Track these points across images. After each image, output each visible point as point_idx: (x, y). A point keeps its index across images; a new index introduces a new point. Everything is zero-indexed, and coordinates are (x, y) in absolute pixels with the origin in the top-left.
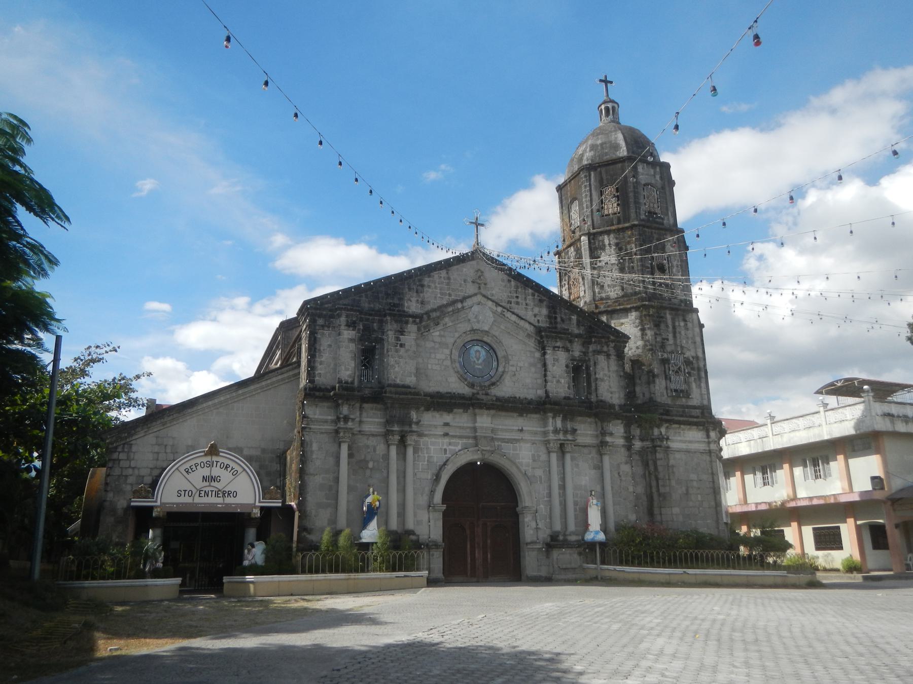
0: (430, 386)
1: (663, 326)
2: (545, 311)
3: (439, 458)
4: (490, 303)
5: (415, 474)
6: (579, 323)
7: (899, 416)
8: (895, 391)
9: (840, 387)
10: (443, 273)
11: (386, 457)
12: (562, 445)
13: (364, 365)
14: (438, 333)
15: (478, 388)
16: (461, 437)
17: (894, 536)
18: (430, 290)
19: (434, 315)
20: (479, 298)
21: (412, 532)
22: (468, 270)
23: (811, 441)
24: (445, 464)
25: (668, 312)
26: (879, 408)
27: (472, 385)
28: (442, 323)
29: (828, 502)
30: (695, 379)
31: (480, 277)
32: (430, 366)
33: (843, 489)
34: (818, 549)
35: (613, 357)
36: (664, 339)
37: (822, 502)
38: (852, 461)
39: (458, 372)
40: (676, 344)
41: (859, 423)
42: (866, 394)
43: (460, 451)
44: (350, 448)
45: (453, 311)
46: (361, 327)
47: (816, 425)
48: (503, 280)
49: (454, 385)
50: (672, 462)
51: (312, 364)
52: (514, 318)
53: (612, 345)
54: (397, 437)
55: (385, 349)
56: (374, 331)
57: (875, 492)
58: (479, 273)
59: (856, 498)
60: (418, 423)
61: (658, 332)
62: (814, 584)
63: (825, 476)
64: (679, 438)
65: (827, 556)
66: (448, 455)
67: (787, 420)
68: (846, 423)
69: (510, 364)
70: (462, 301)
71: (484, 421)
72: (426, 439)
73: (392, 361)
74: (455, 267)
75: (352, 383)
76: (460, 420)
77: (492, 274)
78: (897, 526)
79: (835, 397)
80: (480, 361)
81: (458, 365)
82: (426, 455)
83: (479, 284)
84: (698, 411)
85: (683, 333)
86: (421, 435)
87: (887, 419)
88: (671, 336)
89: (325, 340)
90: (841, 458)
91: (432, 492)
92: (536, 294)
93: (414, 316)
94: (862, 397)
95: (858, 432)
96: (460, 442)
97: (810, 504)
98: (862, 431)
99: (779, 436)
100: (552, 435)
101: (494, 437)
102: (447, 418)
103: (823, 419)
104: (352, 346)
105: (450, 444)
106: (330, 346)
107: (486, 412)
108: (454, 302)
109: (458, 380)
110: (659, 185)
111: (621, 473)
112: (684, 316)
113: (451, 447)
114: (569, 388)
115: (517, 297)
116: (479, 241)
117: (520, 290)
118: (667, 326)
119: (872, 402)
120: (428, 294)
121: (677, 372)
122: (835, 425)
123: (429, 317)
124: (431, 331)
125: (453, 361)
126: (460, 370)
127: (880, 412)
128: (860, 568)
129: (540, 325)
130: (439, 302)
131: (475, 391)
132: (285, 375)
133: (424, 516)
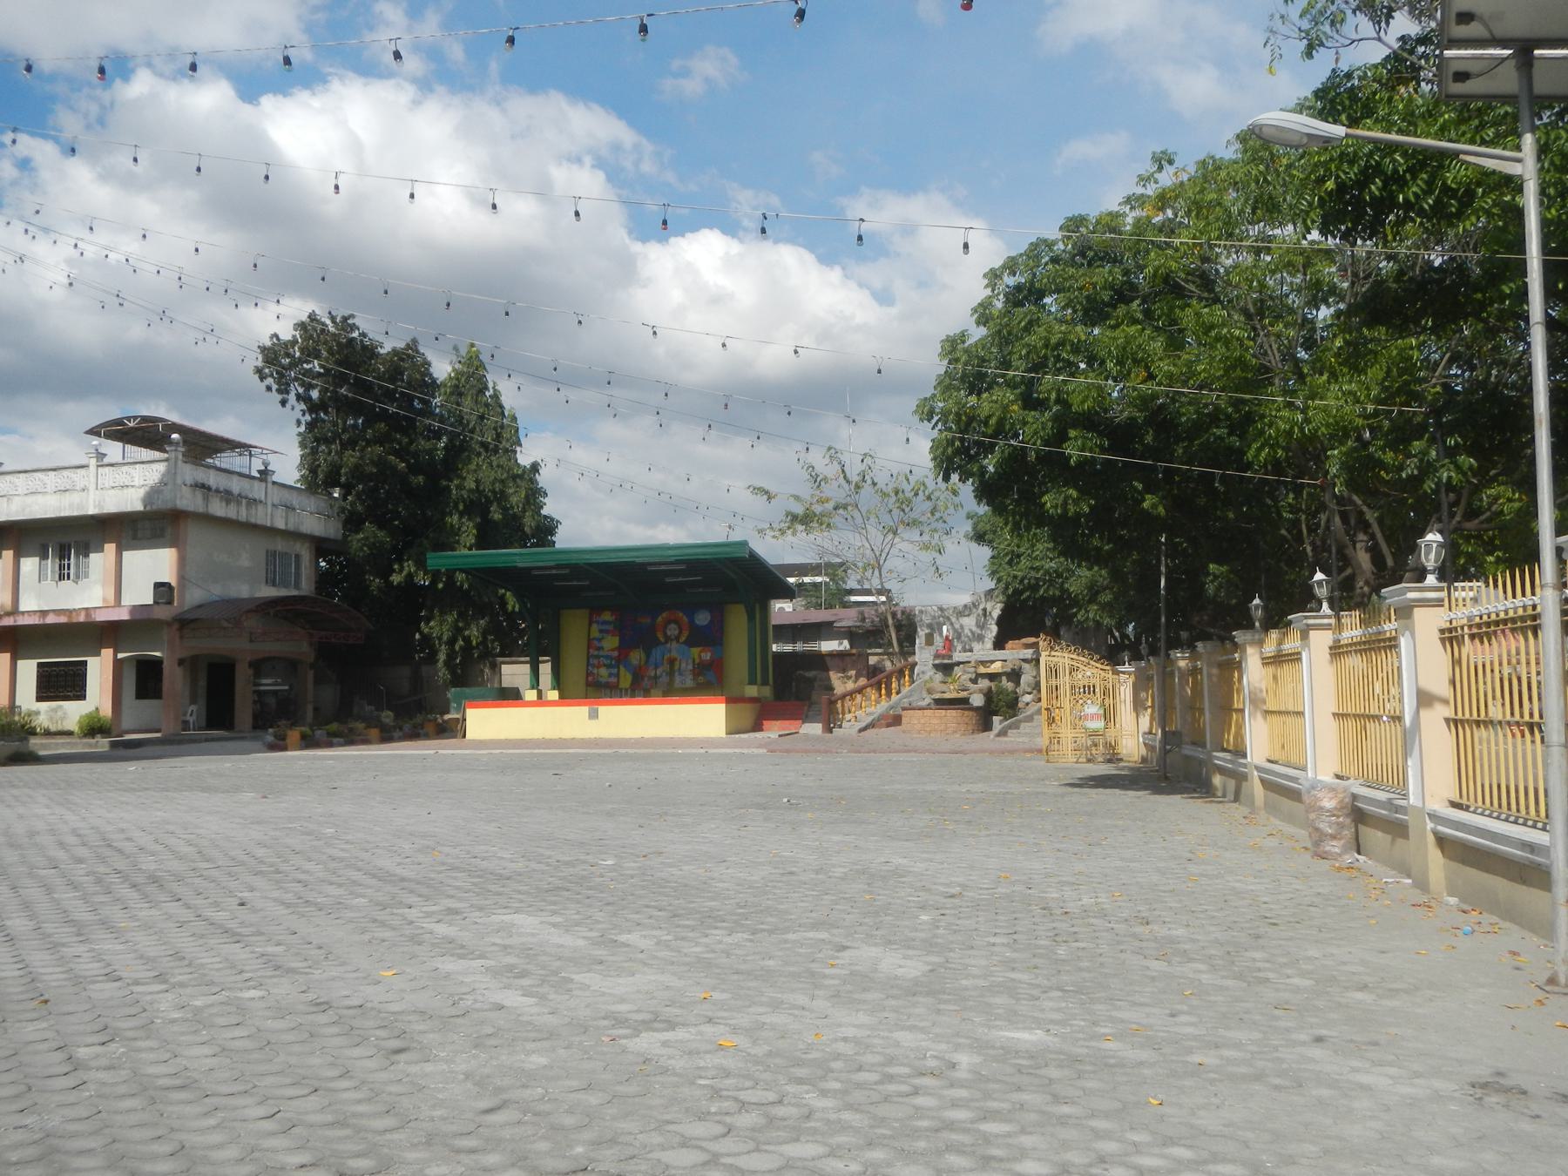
7: (217, 491)
8: (221, 451)
9: (132, 428)
17: (174, 678)
23: (62, 514)
26: (190, 473)
29: (75, 621)
33: (104, 600)
34: (41, 698)
37: (63, 619)
38: (126, 555)
41: (152, 494)
42: (173, 448)
47: (78, 488)
57: (156, 607)
59: (124, 615)
62: (24, 758)
63: (78, 577)
65: (55, 710)
67: (26, 472)
68: (133, 490)
78: (181, 662)
79: (121, 444)
87: (199, 494)
90: (110, 548)
94: (165, 451)
95: (148, 508)
97: (41, 622)
98: (154, 507)
99: (5, 499)
103: (93, 480)
119: (180, 462)
122: (113, 492)
127: (189, 481)
128: (109, 729)
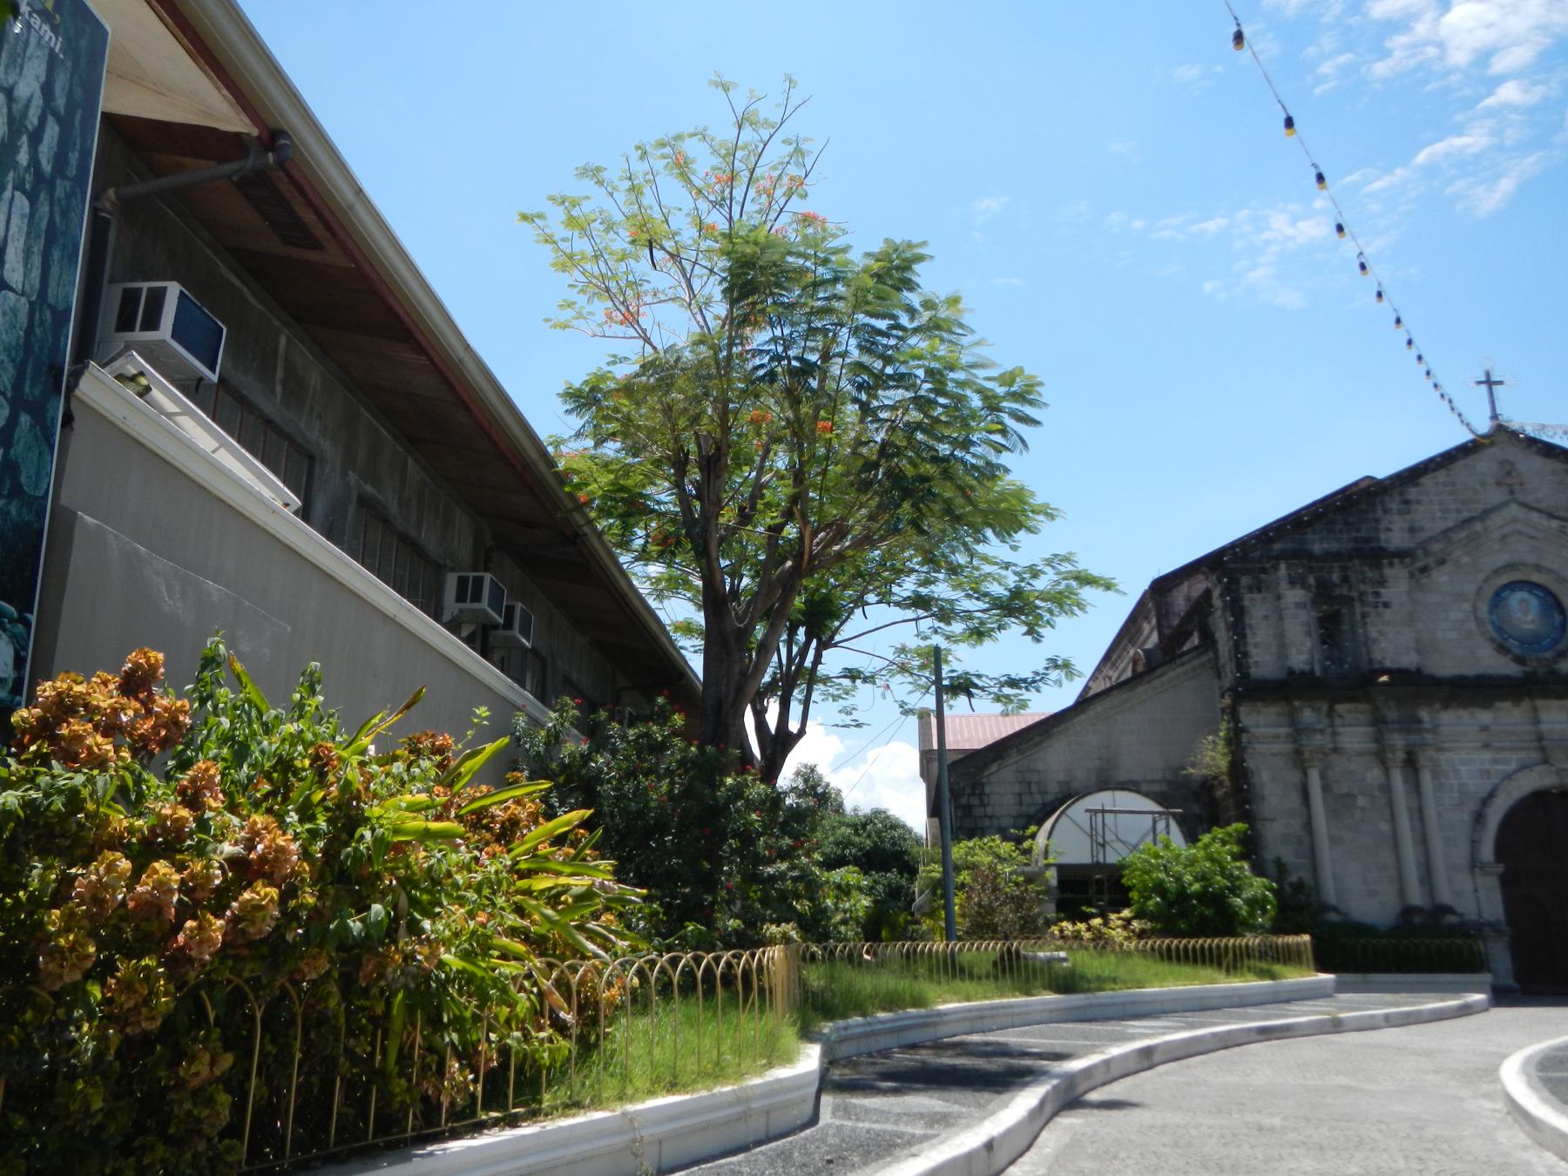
0: (1445, 666)
3: (1478, 787)
4: (1535, 516)
5: (1439, 814)
10: (1441, 476)
11: (1387, 788)
13: (1324, 643)
14: (1445, 578)
15: (1534, 664)
16: (1513, 749)
18: (1422, 508)
19: (1436, 547)
20: (1514, 510)
21: (1450, 910)
22: (1484, 464)
24: (1491, 795)
27: (1520, 660)
31: (1509, 473)
32: (1439, 635)
39: (1493, 640)
43: (1515, 772)
44: (1323, 776)
48: (1554, 473)
49: (1493, 663)
51: (1242, 649)
54: (1401, 755)
55: (1358, 617)
56: (1335, 585)
58: (1508, 467)
60: (1434, 730)
66: (1495, 781)
72: (1448, 755)
73: (1373, 632)
74: (1460, 463)
75: (1312, 671)
76: (1510, 716)
77: (1531, 465)
80: (1530, 617)
81: (1490, 627)
82: (1455, 782)
83: (1509, 485)
86: (1439, 749)
89: (1257, 609)
91: (1475, 843)
93: (1402, 555)
102: (1485, 716)
104: (1304, 615)
105: (1495, 761)
106: (1266, 617)
107: (1555, 703)
108: (1468, 521)
109: (1495, 653)
113: (1499, 767)
116: (1498, 412)
120: (1420, 515)
123: (1427, 553)
125: (1480, 622)
126: (1494, 634)
130: (1441, 526)
131: (1528, 669)
132: (1188, 666)
133: (1464, 881)
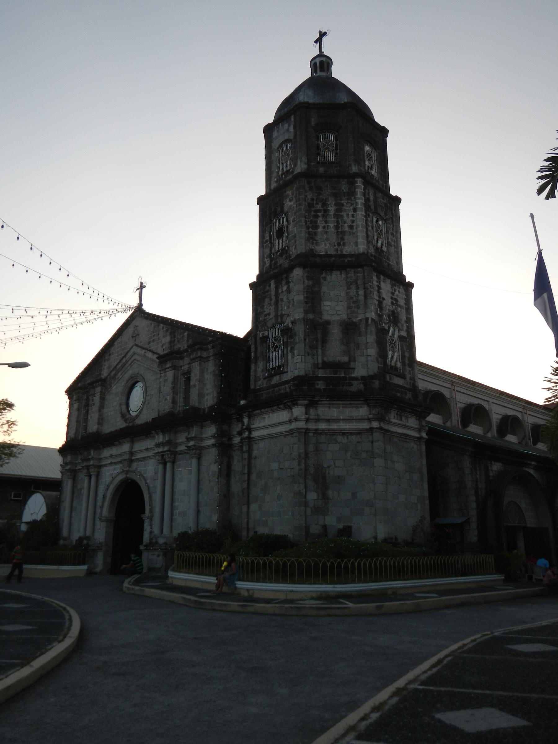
0: (107, 429)
1: (267, 300)
2: (168, 339)
4: (139, 349)
6: (188, 340)
10: (120, 340)
12: (163, 456)
20: (135, 349)
22: (130, 330)
25: (272, 283)
27: (126, 421)
28: (117, 377)
30: (291, 348)
35: (212, 358)
36: (266, 315)
39: (121, 413)
40: (276, 316)
45: (121, 366)
46: (86, 398)
50: (255, 453)
52: (149, 355)
53: (210, 346)
61: (262, 311)
64: (261, 425)
69: (147, 394)
70: (125, 356)
71: (126, 447)
74: (125, 331)
81: (124, 407)
84: (287, 386)
85: (285, 299)
88: (272, 308)
91: (102, 507)
92: (165, 326)
96: (119, 466)
100: (156, 449)
101: (133, 458)
105: (115, 469)
110: (291, 137)
111: (210, 473)
112: (287, 278)
114: (174, 402)
115: (154, 336)
117: (156, 328)
118: (271, 300)
121: (277, 347)
124: (112, 386)
129: (166, 352)
130: (116, 363)
131: (127, 424)
